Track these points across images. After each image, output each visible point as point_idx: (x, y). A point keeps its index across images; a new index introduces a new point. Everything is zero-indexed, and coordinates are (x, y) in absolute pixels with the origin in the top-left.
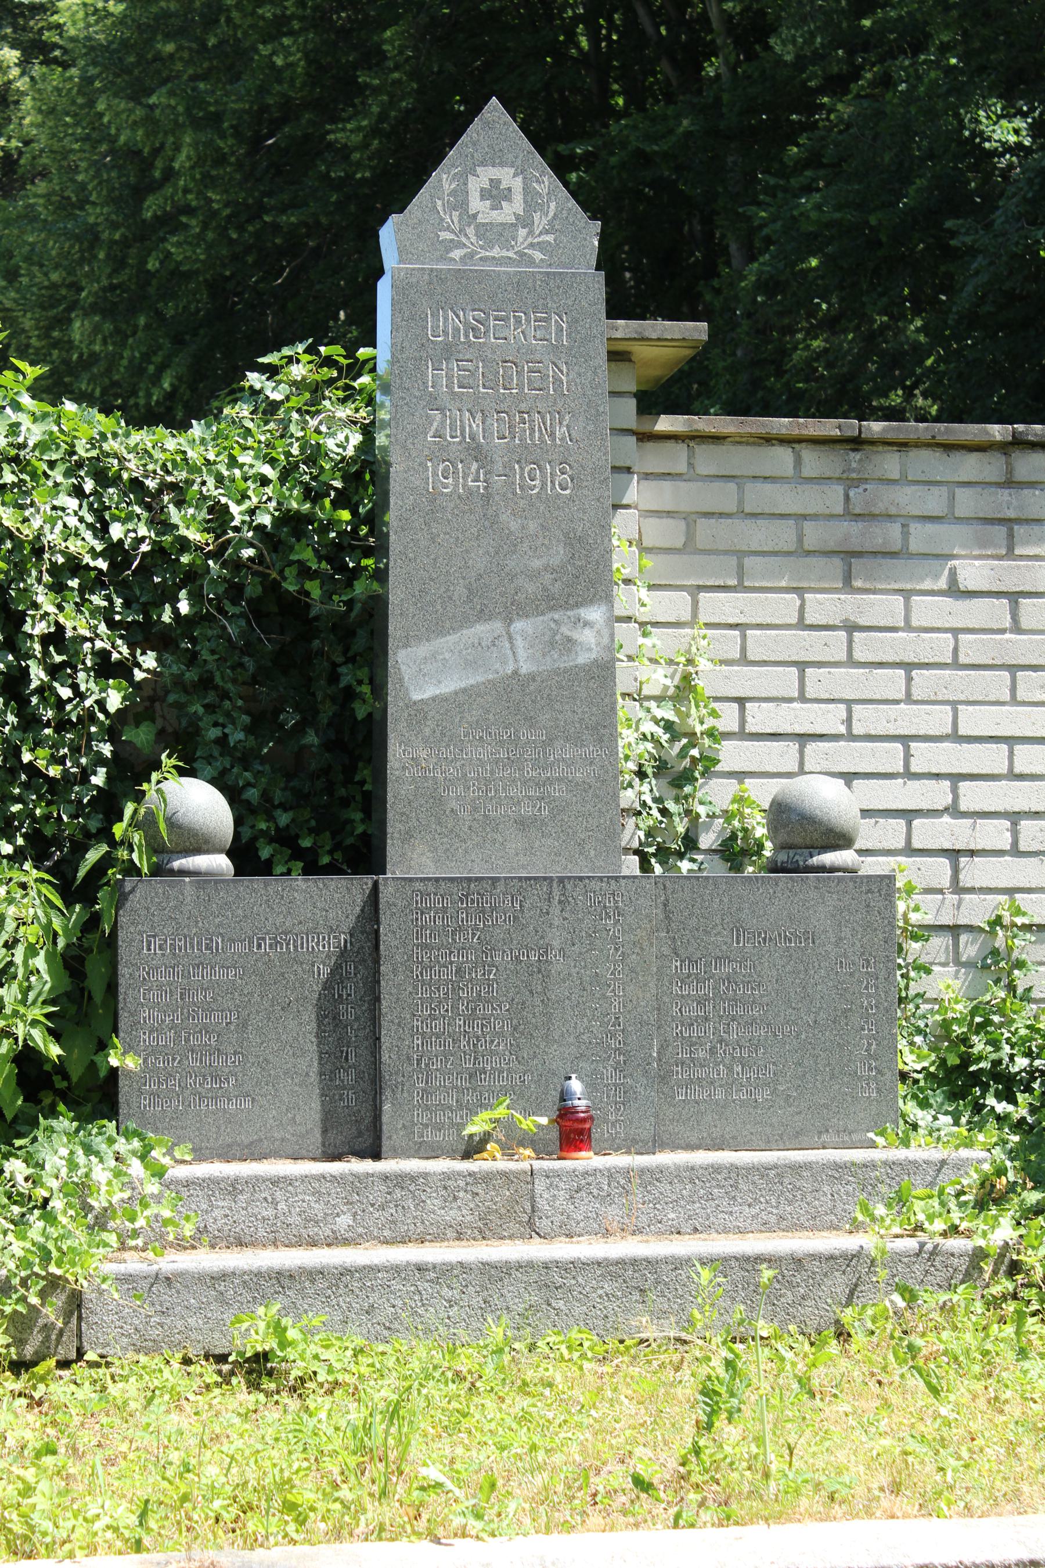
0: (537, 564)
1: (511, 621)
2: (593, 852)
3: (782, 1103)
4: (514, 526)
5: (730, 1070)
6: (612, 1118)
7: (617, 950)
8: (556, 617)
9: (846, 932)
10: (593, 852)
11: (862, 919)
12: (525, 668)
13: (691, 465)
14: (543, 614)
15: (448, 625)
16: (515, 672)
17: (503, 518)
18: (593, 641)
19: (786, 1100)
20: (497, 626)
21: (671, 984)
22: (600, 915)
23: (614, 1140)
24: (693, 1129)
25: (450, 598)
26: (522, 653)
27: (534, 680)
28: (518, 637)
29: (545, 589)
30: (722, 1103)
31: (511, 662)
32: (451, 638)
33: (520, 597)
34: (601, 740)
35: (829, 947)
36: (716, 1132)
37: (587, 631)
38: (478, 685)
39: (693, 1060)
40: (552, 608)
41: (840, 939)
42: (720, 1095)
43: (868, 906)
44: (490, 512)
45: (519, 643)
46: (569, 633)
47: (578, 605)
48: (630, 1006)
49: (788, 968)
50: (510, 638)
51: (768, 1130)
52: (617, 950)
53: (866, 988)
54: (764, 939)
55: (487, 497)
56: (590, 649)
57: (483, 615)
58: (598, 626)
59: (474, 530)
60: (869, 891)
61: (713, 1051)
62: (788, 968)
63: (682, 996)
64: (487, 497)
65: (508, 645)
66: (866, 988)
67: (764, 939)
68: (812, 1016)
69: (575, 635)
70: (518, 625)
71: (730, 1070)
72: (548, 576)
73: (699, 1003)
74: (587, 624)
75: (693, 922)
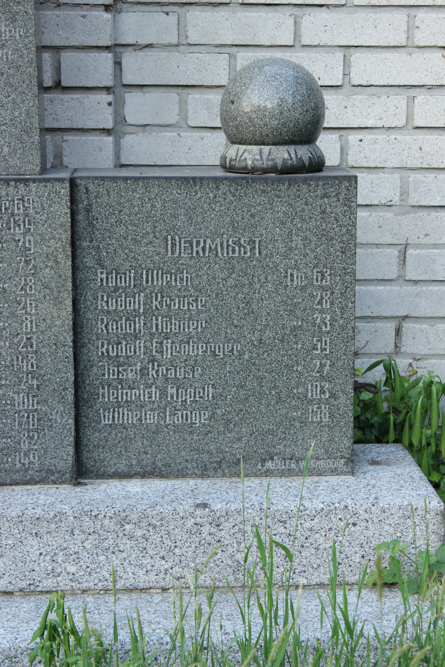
2: (6, 149)
3: (221, 428)
5: (163, 393)
6: (25, 447)
7: (27, 262)
9: (297, 241)
10: (6, 149)
11: (317, 227)
19: (226, 426)
21: (96, 298)
22: (9, 222)
23: (27, 470)
24: (120, 456)
30: (154, 428)
34: (13, 20)
35: (277, 259)
36: (147, 460)
39: (120, 381)
41: (291, 249)
42: (151, 419)
43: (323, 212)
48: (43, 326)
49: (231, 282)
51: (205, 457)
52: (27, 262)
53: (320, 303)
54: (204, 249)
60: (325, 196)
61: (144, 372)
62: (231, 282)
63: (108, 312)
66: (320, 303)
67: (204, 249)
68: (257, 334)
71: (163, 393)
73: (127, 319)
75: (121, 231)
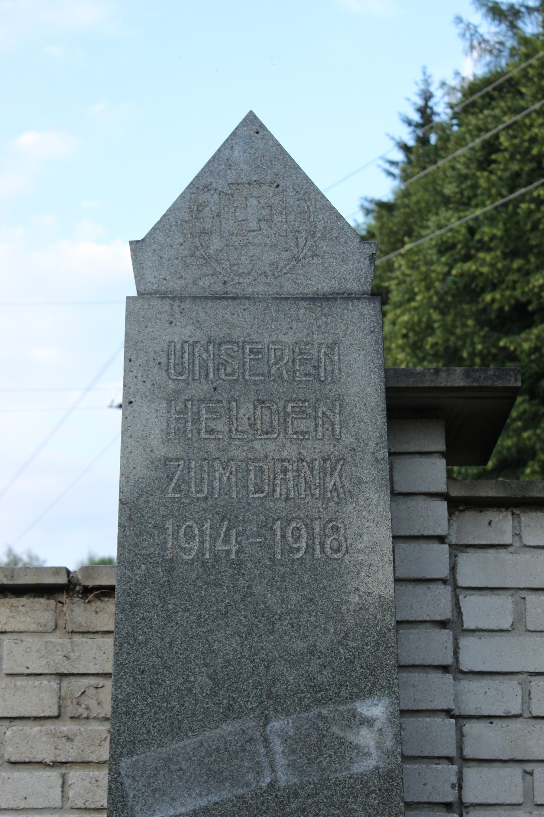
0: (300, 645)
1: (267, 720)
4: (272, 600)
8: (325, 712)
12: (284, 778)
13: (517, 535)
14: (307, 708)
15: (185, 725)
16: (271, 785)
17: (257, 589)
18: (372, 743)
20: (251, 723)
25: (189, 690)
26: (280, 760)
27: (296, 795)
28: (278, 741)
29: (310, 678)
31: (267, 772)
32: (190, 742)
33: (279, 689)
37: (364, 731)
38: (223, 802)
40: (318, 702)
44: (241, 582)
45: (278, 747)
46: (341, 734)
47: (352, 697)
50: (266, 740)
55: (238, 565)
56: (370, 755)
57: (230, 712)
58: (378, 725)
59: (221, 606)
64: (238, 565)
65: (263, 751)
69: (351, 737)
70: (276, 725)
72: (315, 662)
74: (369, 722)
